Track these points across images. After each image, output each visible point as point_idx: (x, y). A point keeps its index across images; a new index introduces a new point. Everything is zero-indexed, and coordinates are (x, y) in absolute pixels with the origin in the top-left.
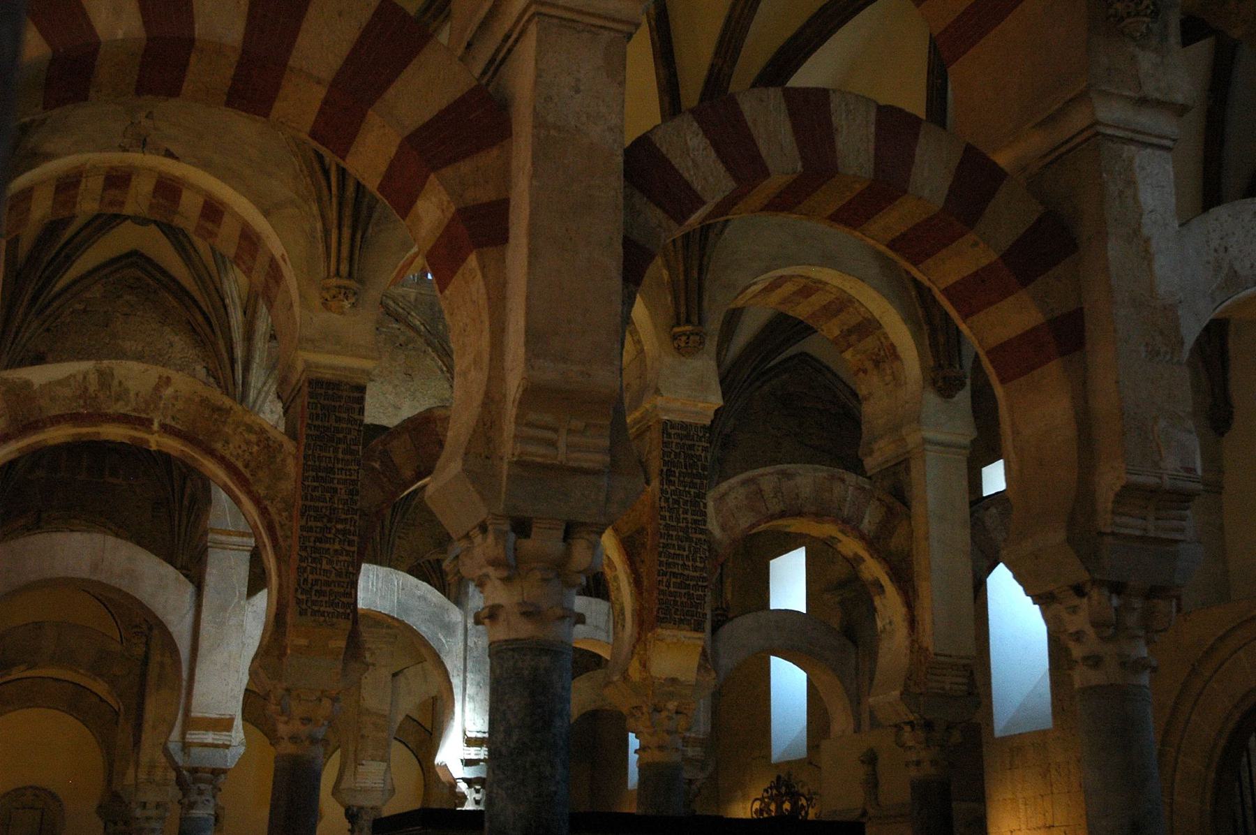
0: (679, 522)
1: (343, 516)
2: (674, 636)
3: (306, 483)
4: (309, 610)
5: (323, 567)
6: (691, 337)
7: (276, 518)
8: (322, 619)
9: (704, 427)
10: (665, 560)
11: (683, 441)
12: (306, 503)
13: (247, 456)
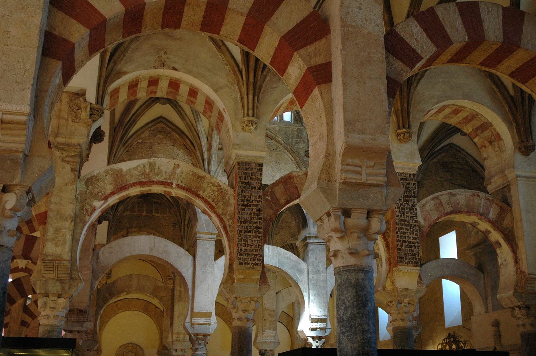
0: (404, 217)
1: (256, 221)
2: (406, 269)
3: (239, 207)
4: (243, 263)
5: (248, 244)
6: (406, 134)
7: (227, 223)
8: (249, 266)
9: (414, 175)
11: (405, 181)
12: (239, 216)
13: (213, 197)
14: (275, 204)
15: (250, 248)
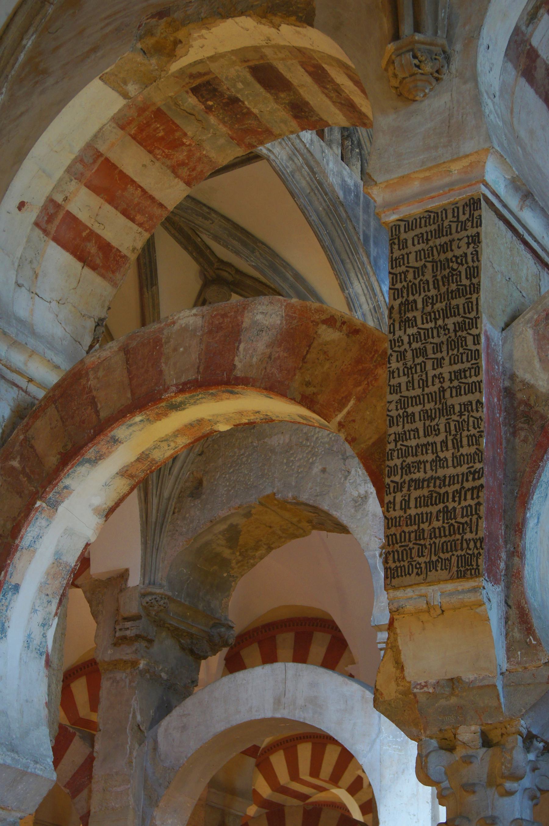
2: (421, 596)
10: (398, 462)
11: (431, 243)
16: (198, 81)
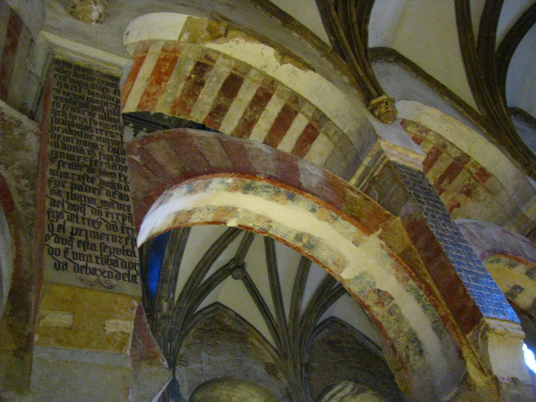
1: (109, 170)
4: (71, 266)
5: (86, 216)
8: (92, 278)
14: (153, 172)
15: (92, 229)
16: (205, 61)
